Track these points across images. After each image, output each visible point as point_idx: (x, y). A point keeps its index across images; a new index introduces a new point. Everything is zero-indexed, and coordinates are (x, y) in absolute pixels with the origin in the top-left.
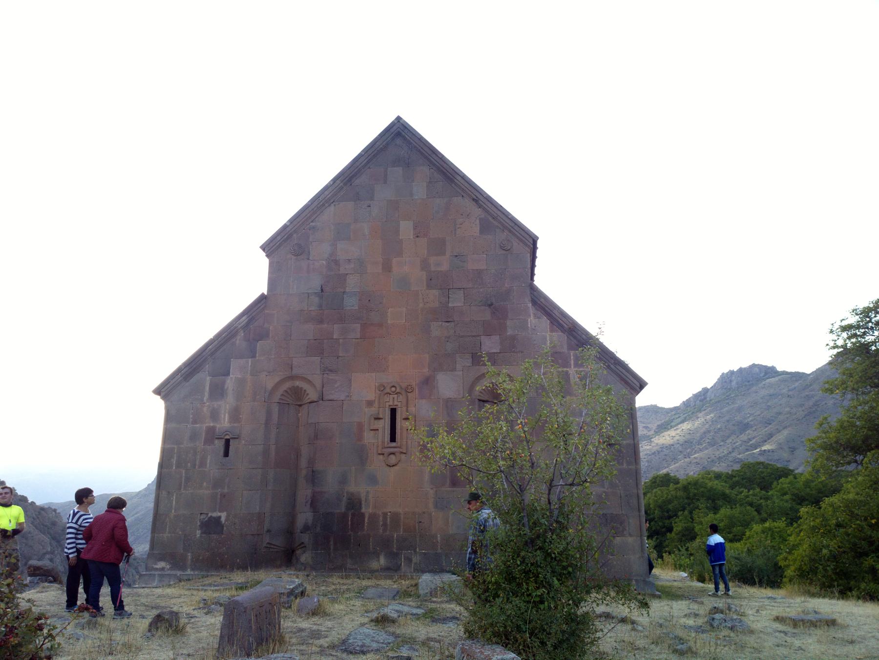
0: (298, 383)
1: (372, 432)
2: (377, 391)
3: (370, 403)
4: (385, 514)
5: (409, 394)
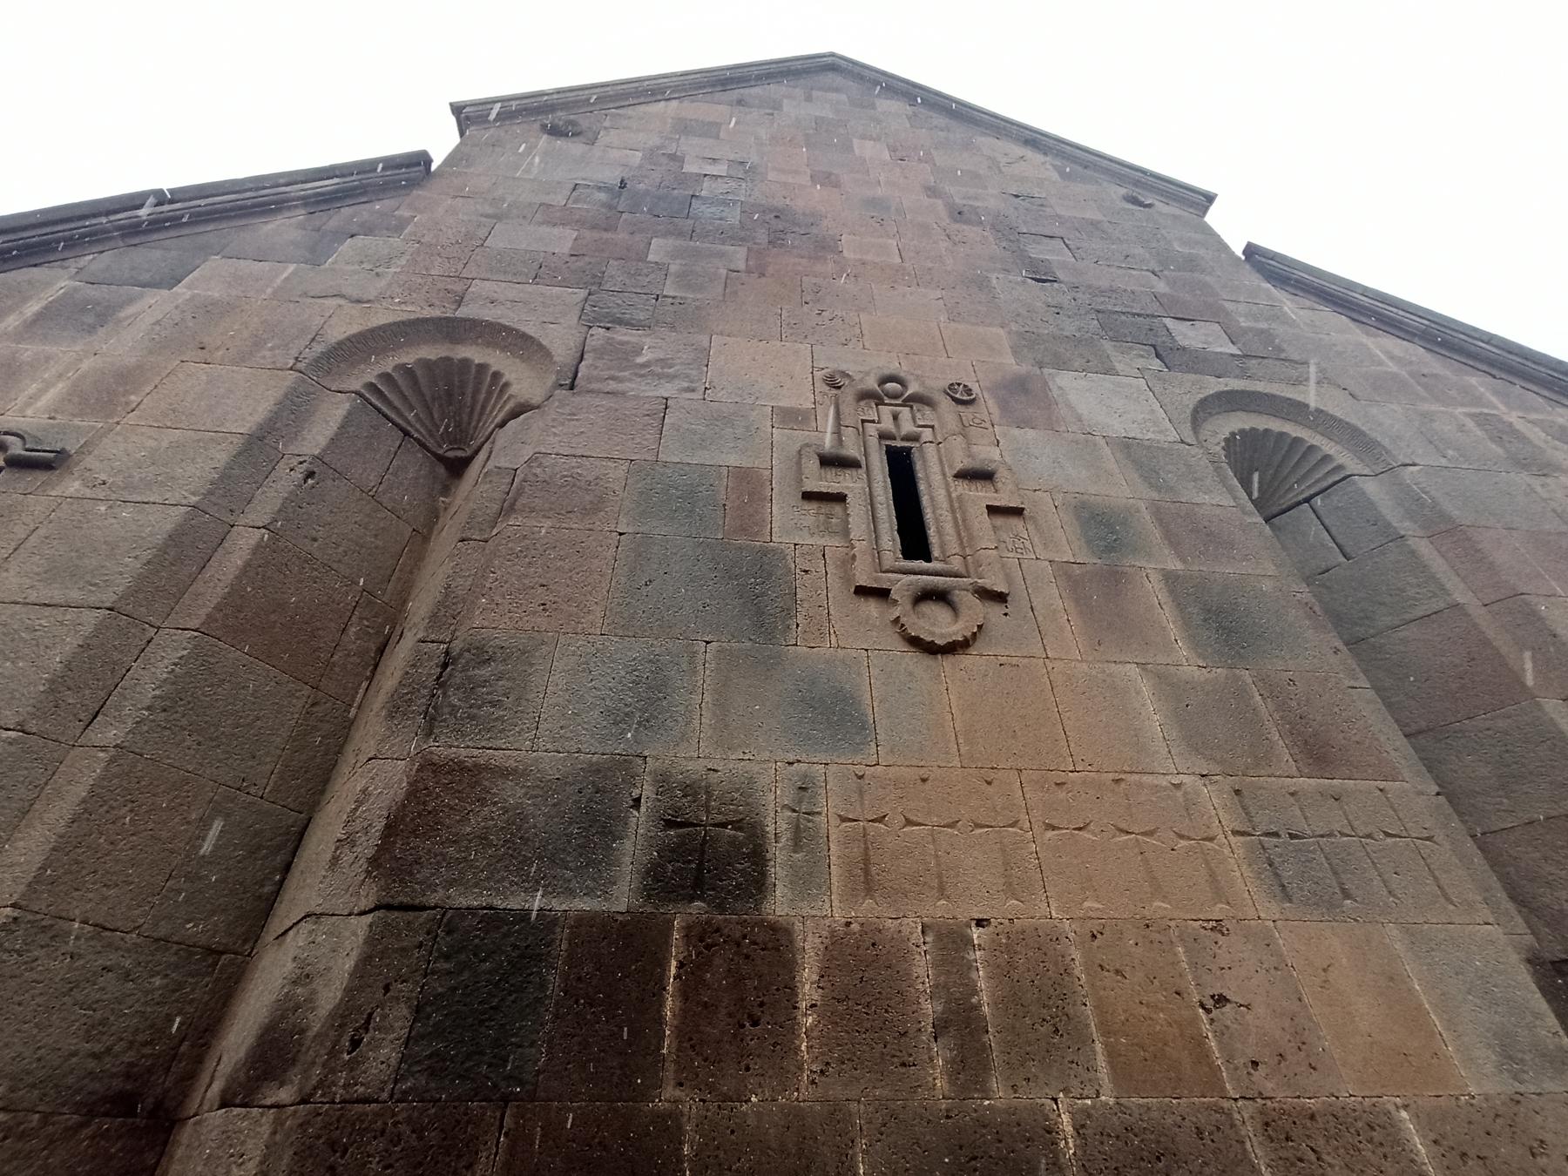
0: (473, 353)
1: (812, 507)
2: (821, 387)
3: (791, 417)
4: (951, 942)
5: (961, 408)
